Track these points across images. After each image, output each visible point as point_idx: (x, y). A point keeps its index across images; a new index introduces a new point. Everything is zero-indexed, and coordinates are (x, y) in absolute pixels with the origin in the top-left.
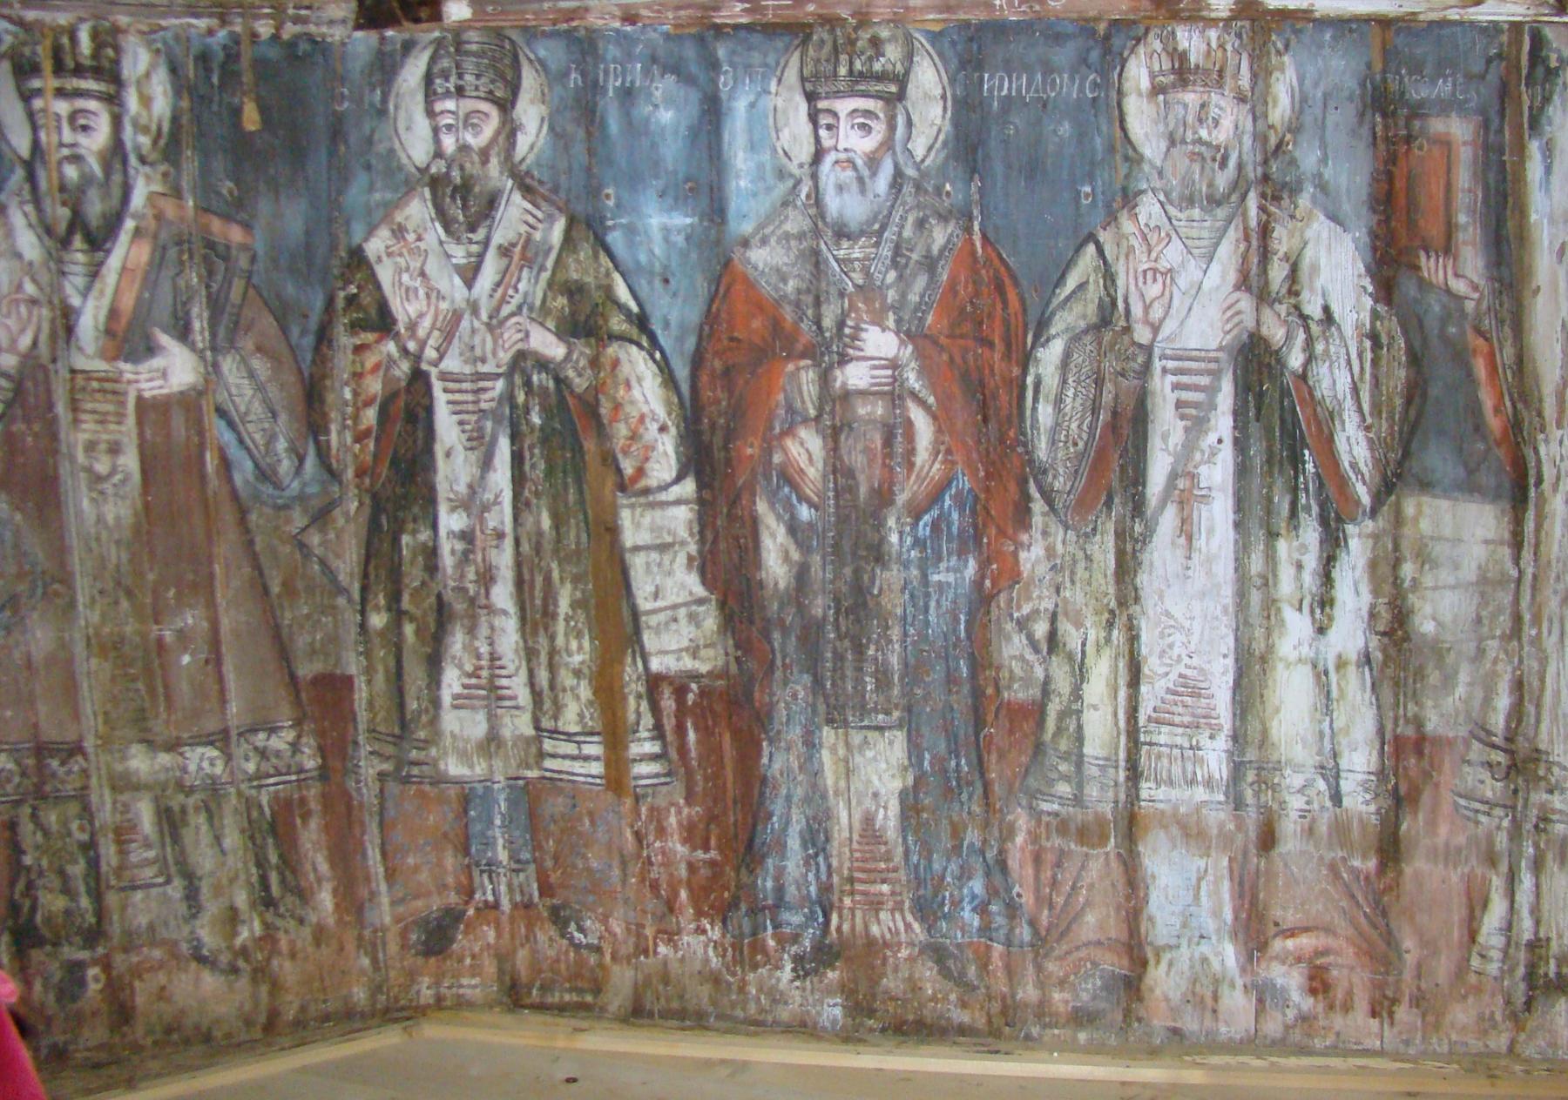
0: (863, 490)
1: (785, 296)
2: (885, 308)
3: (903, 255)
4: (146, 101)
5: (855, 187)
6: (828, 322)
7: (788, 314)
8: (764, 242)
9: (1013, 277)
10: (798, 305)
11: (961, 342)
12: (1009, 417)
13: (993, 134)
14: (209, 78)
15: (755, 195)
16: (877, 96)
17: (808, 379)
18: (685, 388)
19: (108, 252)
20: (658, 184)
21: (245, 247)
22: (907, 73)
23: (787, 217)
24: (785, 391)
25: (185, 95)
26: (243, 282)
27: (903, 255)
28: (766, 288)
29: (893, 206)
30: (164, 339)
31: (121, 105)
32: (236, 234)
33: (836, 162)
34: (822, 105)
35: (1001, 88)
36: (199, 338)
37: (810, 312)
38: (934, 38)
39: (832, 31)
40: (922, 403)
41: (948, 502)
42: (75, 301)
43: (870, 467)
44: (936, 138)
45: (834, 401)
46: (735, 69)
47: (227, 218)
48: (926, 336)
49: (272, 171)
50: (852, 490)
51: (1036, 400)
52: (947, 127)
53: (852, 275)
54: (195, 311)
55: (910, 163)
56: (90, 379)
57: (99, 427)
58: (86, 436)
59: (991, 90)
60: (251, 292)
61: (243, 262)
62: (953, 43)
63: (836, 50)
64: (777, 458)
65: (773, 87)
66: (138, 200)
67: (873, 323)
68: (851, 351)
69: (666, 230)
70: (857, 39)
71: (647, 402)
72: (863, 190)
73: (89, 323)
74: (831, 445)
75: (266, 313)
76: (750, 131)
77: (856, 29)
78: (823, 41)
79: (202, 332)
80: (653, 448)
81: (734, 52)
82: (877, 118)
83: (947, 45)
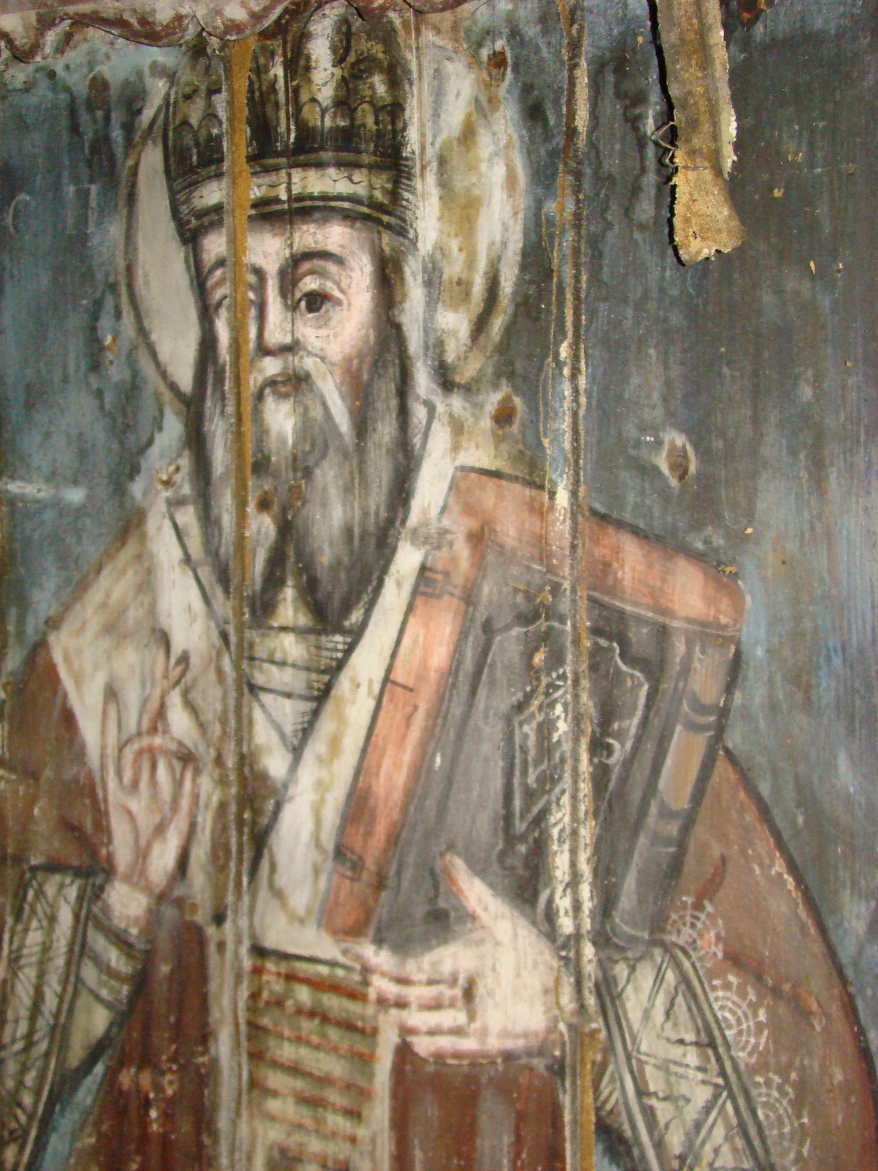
4: (463, 210)
14: (634, 122)
19: (357, 634)
21: (707, 633)
25: (565, 180)
26: (701, 742)
30: (476, 893)
31: (401, 231)
32: (688, 594)
36: (563, 903)
42: (276, 764)
47: (662, 542)
49: (806, 392)
54: (560, 818)
56: (291, 978)
57: (305, 1116)
58: (274, 1134)
60: (723, 770)
61: (705, 680)
66: (430, 491)
73: (303, 823)
75: (763, 843)
79: (574, 882)
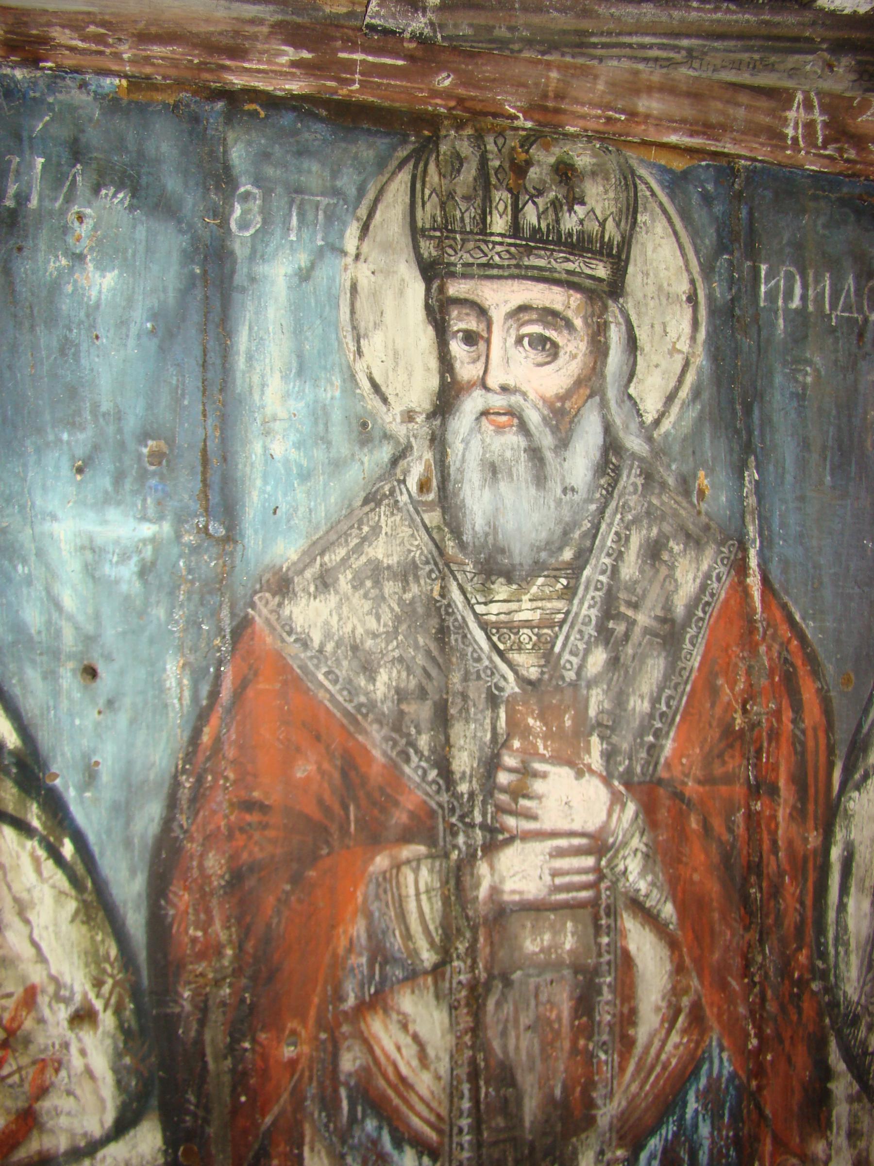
0: (531, 1107)
1: (372, 705)
2: (582, 730)
3: (620, 617)
5: (523, 468)
6: (463, 761)
7: (376, 743)
8: (325, 582)
9: (812, 659)
10: (398, 724)
11: (723, 789)
12: (800, 929)
13: (778, 379)
15: (305, 476)
16: (569, 283)
17: (419, 886)
18: (136, 922)
20: (81, 440)
22: (627, 242)
23: (376, 529)
24: (369, 916)
27: (620, 617)
28: (326, 686)
29: (602, 511)
33: (485, 413)
34: (456, 288)
35: (789, 295)
37: (424, 741)
38: (676, 183)
39: (479, 138)
40: (649, 917)
41: (692, 1104)
43: (546, 1057)
44: (680, 381)
45: (474, 929)
46: (267, 194)
48: (660, 782)
50: (509, 1107)
51: (844, 890)
52: (700, 359)
53: (517, 657)
55: (634, 426)
59: (772, 296)
62: (707, 199)
63: (484, 183)
64: (350, 1062)
65: (351, 243)
67: (558, 760)
68: (511, 822)
69: (92, 552)
70: (529, 163)
71: (41, 958)
72: (540, 479)
74: (466, 1021)
76: (298, 331)
77: (527, 142)
78: (458, 160)
80: (59, 1065)
81: (266, 156)
82: (569, 325)
83: (695, 200)
